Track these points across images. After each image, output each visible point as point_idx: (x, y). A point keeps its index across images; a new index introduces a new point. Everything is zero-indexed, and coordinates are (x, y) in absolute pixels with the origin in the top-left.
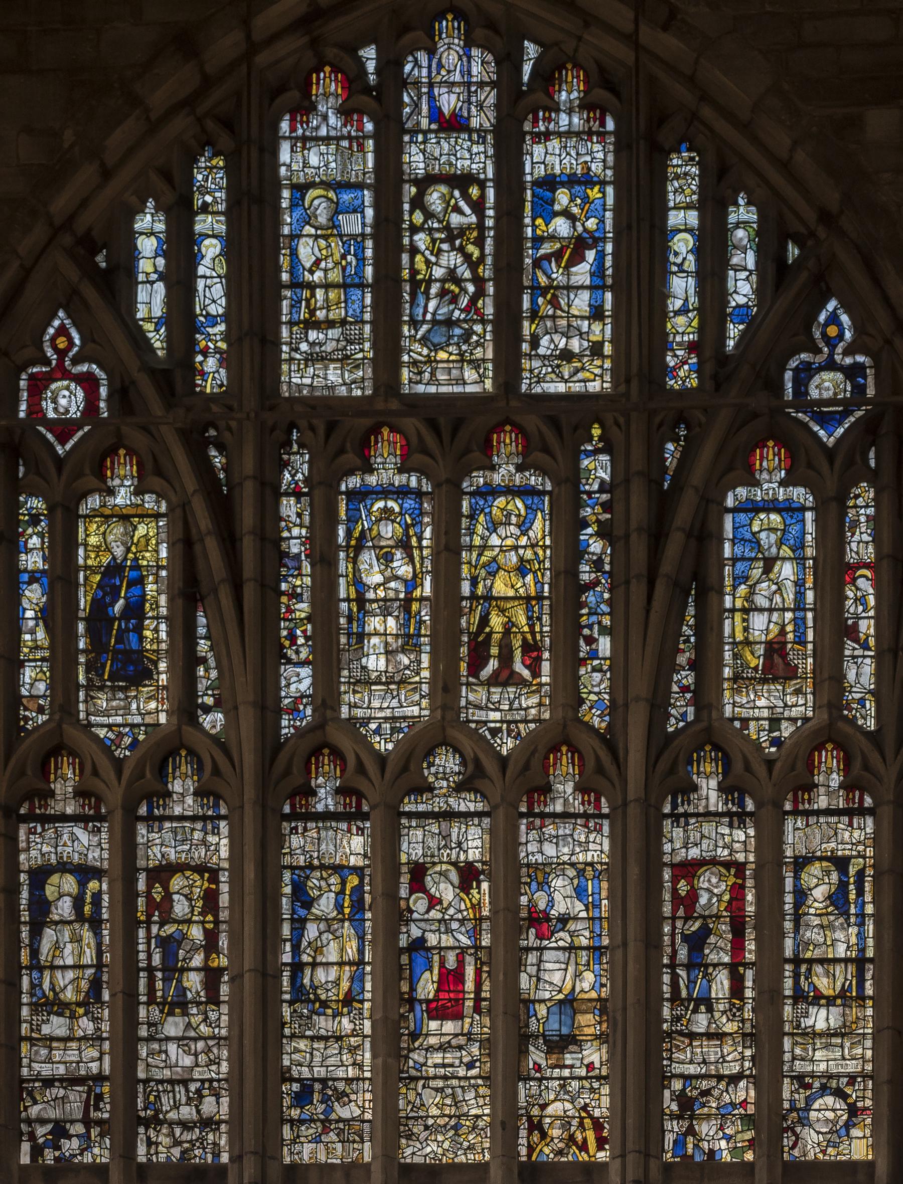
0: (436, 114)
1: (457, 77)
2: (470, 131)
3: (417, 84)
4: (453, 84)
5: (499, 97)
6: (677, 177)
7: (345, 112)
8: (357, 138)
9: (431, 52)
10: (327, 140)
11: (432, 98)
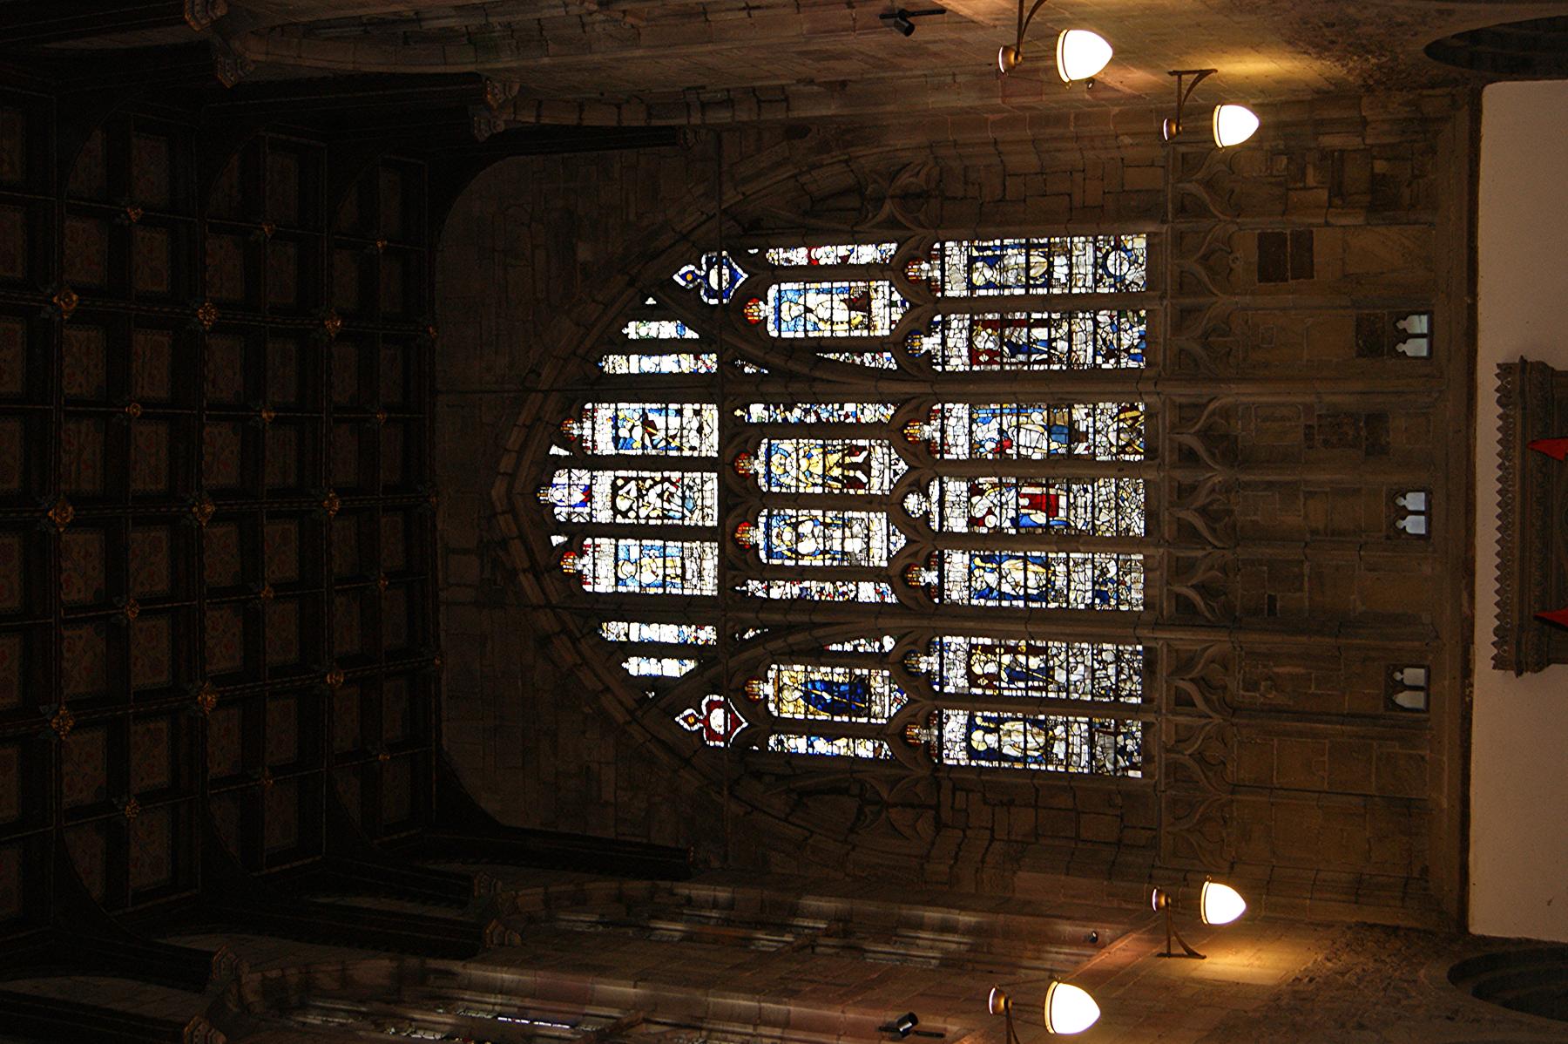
0: (583, 504)
1: (566, 492)
2: (591, 484)
3: (569, 514)
4: (569, 494)
5: (575, 468)
6: (614, 368)
7: (582, 554)
8: (594, 548)
9: (555, 505)
10: (595, 564)
11: (574, 506)
